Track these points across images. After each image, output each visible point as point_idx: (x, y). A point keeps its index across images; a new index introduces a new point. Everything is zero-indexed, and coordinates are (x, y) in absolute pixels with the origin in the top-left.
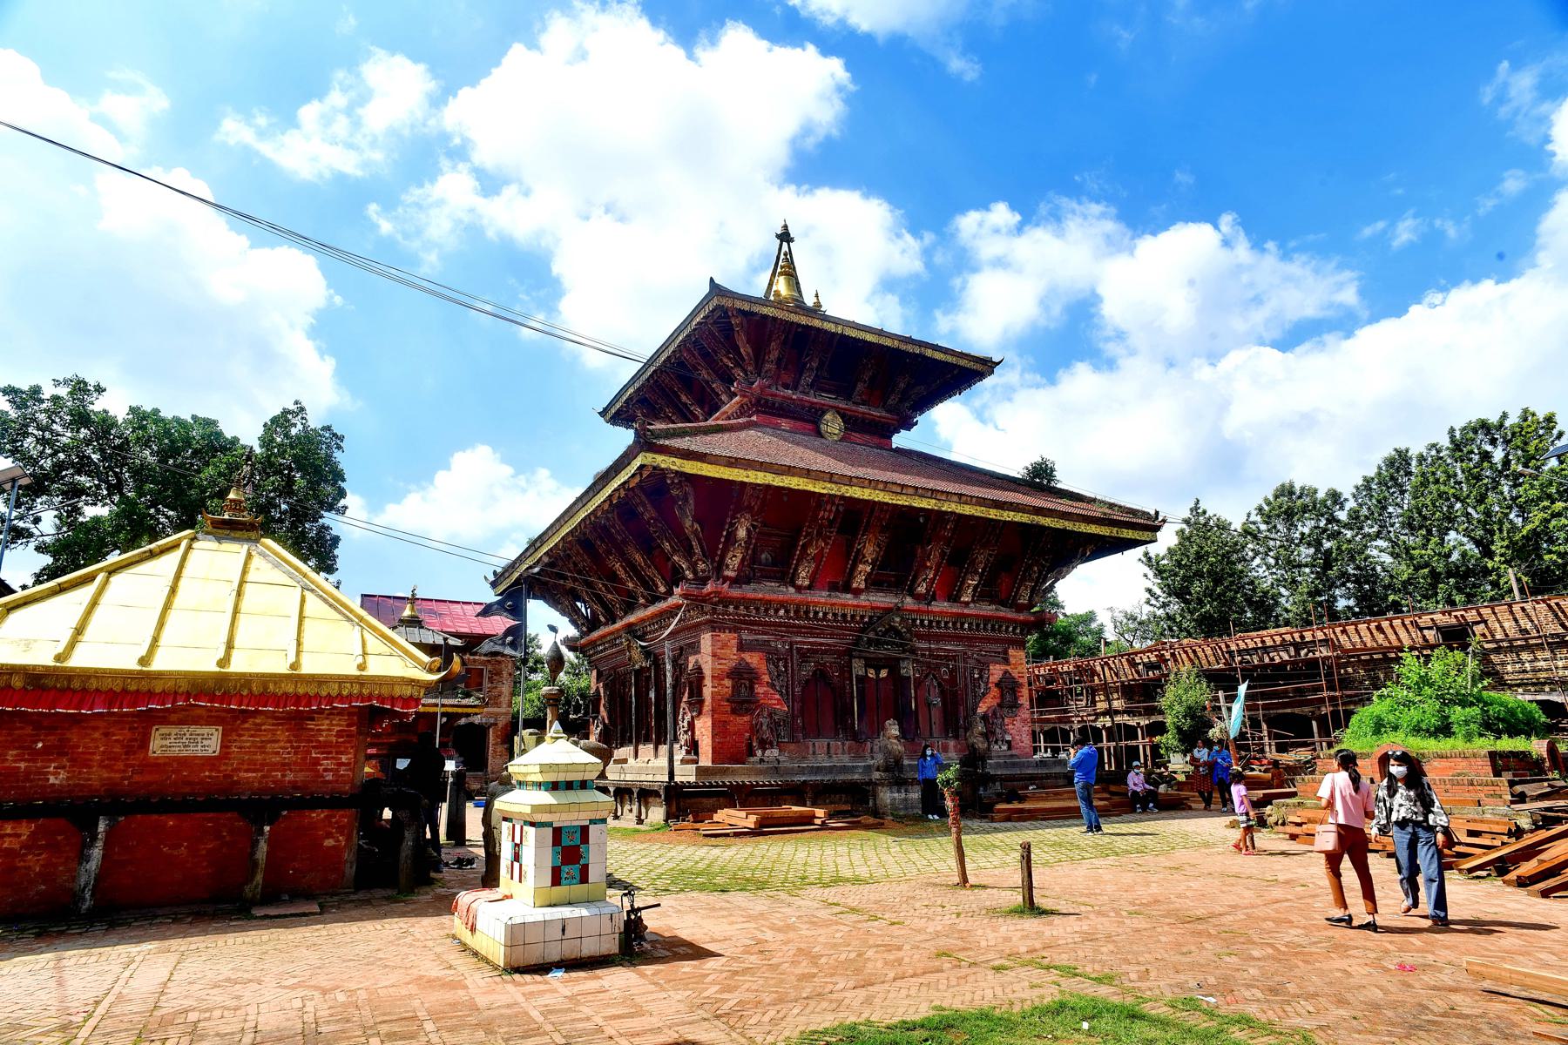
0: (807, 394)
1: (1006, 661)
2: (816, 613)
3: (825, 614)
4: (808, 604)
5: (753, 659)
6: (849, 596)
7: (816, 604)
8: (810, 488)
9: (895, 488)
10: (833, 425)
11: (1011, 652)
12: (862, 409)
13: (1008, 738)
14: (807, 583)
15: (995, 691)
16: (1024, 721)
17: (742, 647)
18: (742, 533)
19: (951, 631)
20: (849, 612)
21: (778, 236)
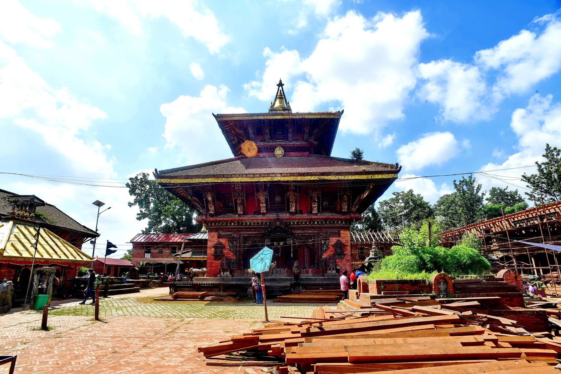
0: (269, 142)
1: (339, 235)
2: (246, 223)
3: (250, 223)
4: (242, 220)
5: (223, 241)
6: (260, 216)
7: (245, 220)
8: (216, 181)
9: (251, 176)
10: (279, 152)
11: (342, 232)
12: (293, 143)
13: (338, 268)
14: (242, 213)
15: (332, 248)
16: (348, 261)
17: (219, 237)
18: (210, 199)
19: (310, 225)
20: (260, 222)
21: (277, 85)
